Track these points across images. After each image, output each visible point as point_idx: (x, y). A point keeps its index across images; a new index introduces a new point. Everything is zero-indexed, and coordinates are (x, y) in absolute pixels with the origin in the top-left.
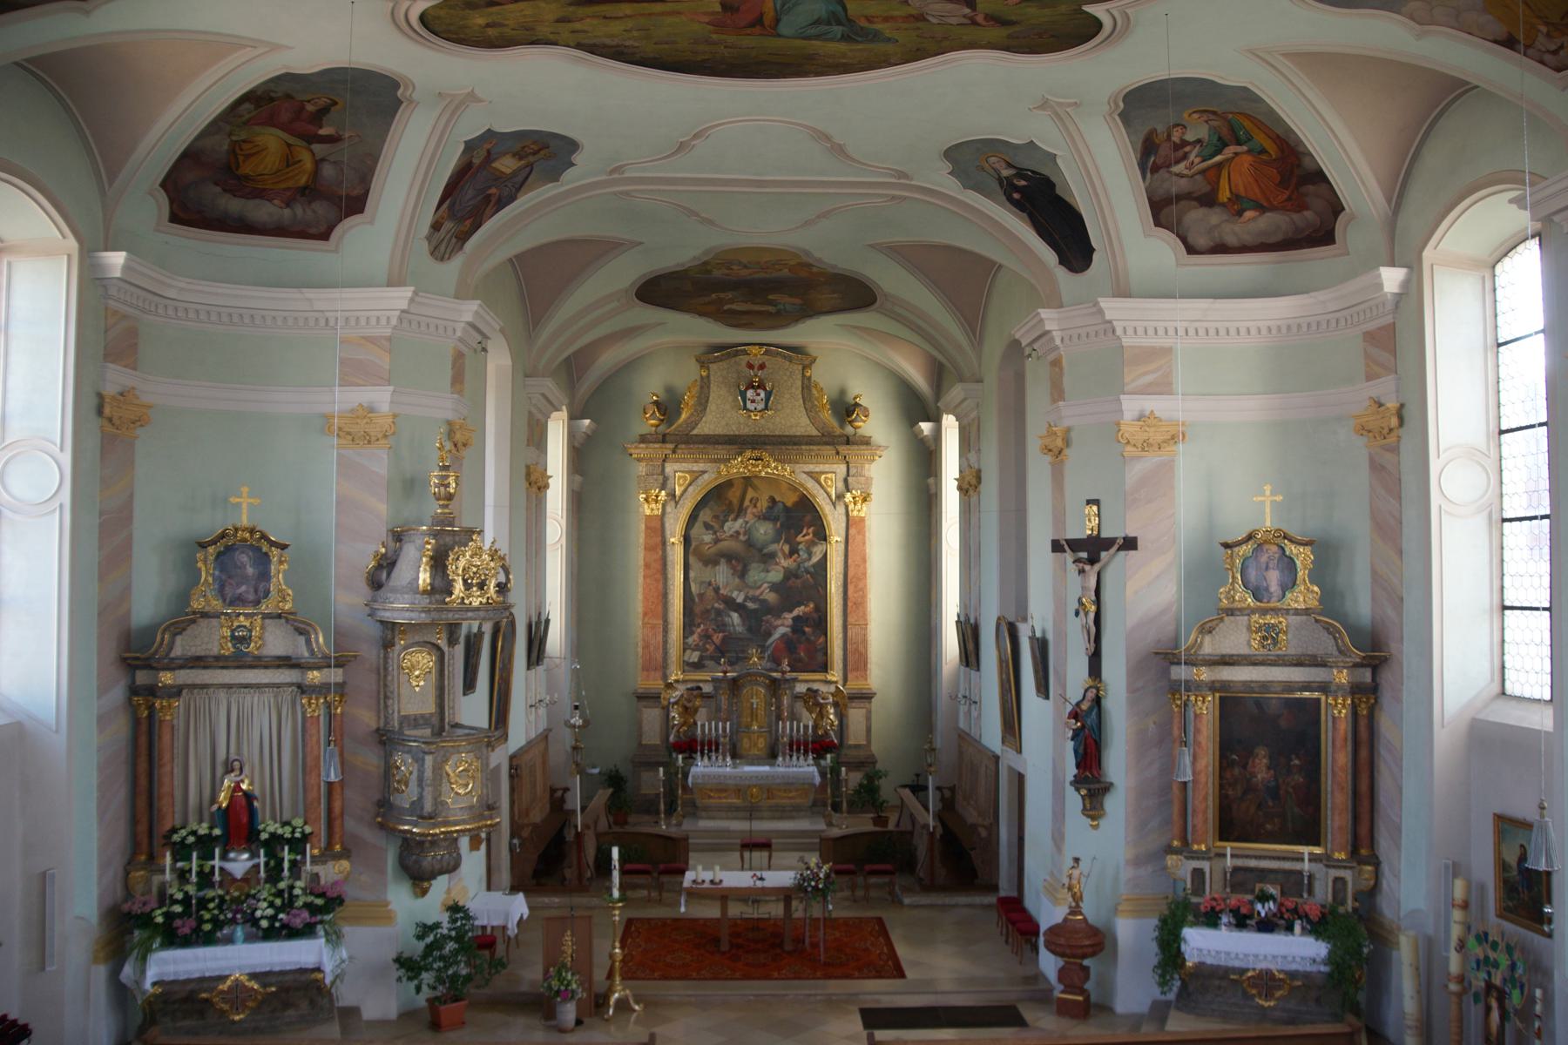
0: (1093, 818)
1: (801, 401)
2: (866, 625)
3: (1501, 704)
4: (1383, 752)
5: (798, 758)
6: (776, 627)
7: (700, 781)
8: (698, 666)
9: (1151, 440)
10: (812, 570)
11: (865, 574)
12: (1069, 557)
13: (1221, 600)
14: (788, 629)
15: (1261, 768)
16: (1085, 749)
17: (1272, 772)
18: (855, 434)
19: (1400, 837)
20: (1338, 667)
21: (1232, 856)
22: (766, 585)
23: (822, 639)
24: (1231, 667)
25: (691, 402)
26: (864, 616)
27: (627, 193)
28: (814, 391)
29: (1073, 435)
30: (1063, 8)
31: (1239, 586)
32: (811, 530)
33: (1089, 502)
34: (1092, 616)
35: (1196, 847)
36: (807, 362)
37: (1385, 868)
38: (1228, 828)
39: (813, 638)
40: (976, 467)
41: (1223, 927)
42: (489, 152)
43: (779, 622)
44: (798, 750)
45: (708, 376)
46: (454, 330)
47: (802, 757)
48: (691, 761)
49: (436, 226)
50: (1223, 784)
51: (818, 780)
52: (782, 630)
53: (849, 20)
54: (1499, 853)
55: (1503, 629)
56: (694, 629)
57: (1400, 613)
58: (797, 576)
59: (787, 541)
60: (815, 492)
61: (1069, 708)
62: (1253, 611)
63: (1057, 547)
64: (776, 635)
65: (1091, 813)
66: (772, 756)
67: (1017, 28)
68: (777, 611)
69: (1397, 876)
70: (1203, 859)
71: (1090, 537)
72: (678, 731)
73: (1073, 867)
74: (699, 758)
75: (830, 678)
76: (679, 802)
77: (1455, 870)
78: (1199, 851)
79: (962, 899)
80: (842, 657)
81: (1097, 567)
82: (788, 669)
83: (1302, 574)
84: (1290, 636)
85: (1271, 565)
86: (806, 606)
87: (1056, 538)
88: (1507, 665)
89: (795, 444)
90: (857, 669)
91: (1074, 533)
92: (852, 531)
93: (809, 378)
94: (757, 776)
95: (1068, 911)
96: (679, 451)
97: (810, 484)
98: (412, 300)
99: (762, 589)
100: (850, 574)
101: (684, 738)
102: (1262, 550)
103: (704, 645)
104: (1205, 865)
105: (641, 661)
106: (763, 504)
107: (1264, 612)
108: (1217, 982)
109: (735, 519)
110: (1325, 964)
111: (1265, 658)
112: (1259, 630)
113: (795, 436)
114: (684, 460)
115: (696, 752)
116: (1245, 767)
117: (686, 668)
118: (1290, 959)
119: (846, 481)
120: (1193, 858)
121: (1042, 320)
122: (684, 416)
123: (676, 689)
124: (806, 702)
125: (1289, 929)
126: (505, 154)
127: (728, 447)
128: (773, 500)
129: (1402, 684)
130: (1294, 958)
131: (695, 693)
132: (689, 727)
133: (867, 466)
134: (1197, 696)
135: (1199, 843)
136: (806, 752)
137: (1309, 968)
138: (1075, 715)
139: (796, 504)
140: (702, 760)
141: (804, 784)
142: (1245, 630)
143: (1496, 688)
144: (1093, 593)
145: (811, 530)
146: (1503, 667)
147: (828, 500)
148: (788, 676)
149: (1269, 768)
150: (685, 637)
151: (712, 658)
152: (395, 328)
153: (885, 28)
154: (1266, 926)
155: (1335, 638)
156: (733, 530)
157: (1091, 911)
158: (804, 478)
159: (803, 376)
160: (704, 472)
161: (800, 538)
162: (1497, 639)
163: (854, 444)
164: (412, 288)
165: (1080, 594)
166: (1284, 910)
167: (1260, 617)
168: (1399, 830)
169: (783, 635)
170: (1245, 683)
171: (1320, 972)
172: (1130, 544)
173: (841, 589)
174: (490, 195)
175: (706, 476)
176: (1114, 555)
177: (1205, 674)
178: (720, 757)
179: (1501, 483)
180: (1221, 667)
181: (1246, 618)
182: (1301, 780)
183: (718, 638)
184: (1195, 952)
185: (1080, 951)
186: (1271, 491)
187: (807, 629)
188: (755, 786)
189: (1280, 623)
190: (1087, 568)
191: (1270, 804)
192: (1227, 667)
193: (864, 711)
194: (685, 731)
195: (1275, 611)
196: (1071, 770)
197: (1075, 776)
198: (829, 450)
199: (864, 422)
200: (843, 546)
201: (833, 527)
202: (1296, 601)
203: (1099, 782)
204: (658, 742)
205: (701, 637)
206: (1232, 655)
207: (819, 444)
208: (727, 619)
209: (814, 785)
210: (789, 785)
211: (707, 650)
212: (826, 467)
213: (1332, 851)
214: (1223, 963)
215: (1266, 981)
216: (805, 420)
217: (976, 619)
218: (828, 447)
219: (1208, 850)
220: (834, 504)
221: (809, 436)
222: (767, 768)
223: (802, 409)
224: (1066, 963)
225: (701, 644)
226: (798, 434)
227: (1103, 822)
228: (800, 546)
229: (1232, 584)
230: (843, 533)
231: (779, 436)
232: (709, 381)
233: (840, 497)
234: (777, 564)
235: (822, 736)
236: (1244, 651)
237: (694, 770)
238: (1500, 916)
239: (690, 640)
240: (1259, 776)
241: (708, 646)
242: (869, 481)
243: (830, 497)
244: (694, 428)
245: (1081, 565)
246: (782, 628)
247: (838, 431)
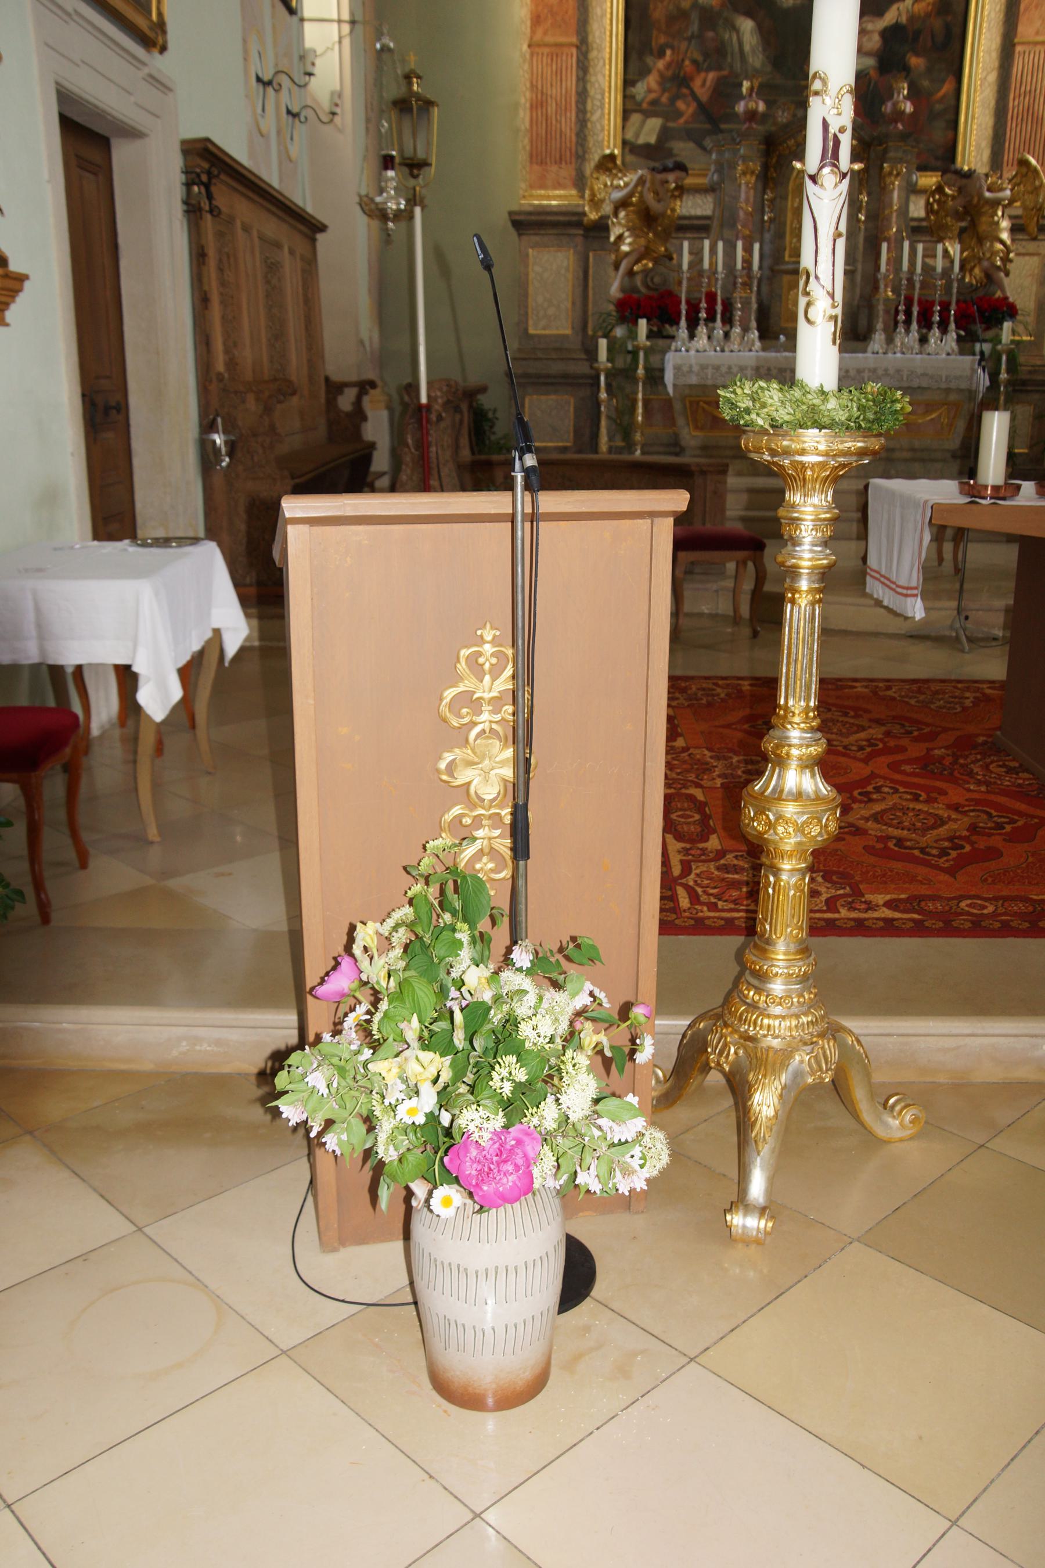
5: (923, 340)
39: (926, 83)
44: (926, 322)
47: (936, 332)
48: (661, 342)
56: (649, 60)
72: (631, 273)
74: (683, 332)
76: (638, 437)
80: (989, 132)
101: (643, 290)
103: (673, 100)
105: (526, 141)
115: (676, 322)
132: (656, 261)
140: (692, 336)
141: (948, 391)
150: (628, 83)
178: (737, 330)
183: (704, 84)
193: (1036, 259)
194: (646, 272)
204: (568, 332)
205: (663, 80)
211: (679, 114)
225: (664, 99)
237: (671, 360)
239: (640, 90)
241: (681, 105)
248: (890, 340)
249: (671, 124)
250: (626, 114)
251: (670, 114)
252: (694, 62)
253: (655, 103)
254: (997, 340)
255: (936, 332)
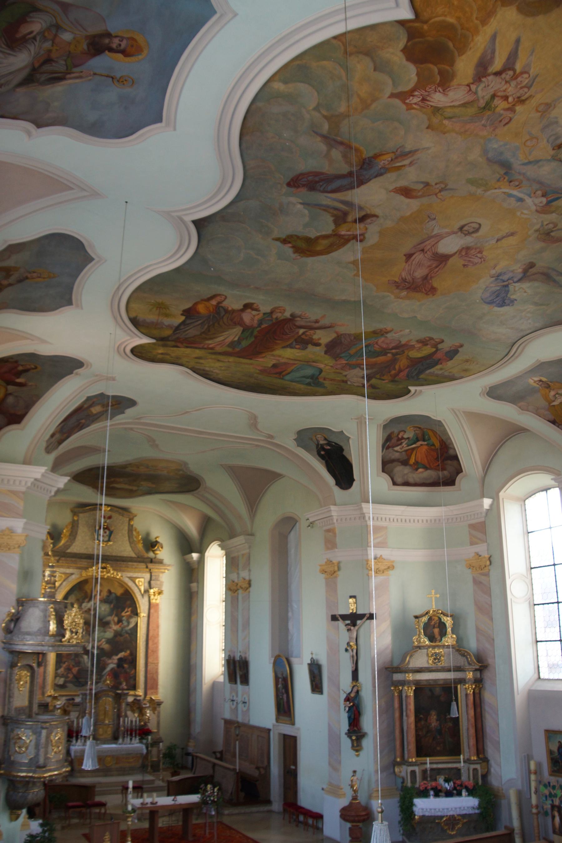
0: (357, 751)
1: (127, 538)
2: (158, 663)
3: (539, 682)
4: (487, 708)
5: (131, 739)
6: (108, 664)
7: (78, 754)
8: (62, 687)
9: (380, 569)
10: (129, 632)
11: (158, 635)
12: (341, 624)
13: (414, 642)
14: (115, 666)
15: (433, 720)
16: (354, 716)
17: (438, 722)
18: (155, 558)
19: (499, 747)
20: (468, 671)
21: (430, 763)
22: (104, 640)
23: (133, 672)
24: (421, 674)
25: (68, 534)
26: (157, 658)
27: (132, 429)
28: (134, 533)
29: (341, 565)
30: (401, 386)
31: (422, 636)
32: (130, 609)
33: (351, 597)
34: (355, 651)
35: (410, 760)
36: (131, 517)
37: (492, 762)
38: (421, 751)
39: (128, 671)
40: (247, 578)
41: (432, 797)
42: (93, 403)
43: (110, 661)
44: (131, 735)
45: (78, 520)
46: (51, 491)
49: (52, 436)
50: (417, 729)
51: (145, 751)
52: (111, 666)
53: (317, 378)
54: (548, 747)
55: (537, 651)
57: (493, 645)
58: (121, 635)
59: (116, 615)
60: (133, 588)
61: (344, 696)
62: (429, 647)
63: (334, 618)
64: (108, 669)
65: (357, 748)
66: (115, 738)
67: (377, 390)
68: (109, 655)
69: (499, 765)
70: (415, 765)
71: (352, 614)
73: (353, 776)
74: (74, 741)
75: (137, 693)
77: (529, 758)
78: (412, 762)
79: (254, 809)
81: (357, 628)
82: (125, 687)
83: (449, 630)
84: (445, 658)
85: (436, 626)
86: (125, 652)
87: (334, 614)
88: (540, 666)
89: (123, 561)
90: (152, 688)
91: (342, 611)
92: (152, 611)
93: (132, 526)
94: (111, 750)
95: (351, 798)
96: (61, 561)
97: (130, 584)
98: (43, 475)
99: (101, 642)
100: (151, 634)
102: (432, 620)
104: (416, 769)
106: (105, 594)
107: (434, 647)
108: (430, 825)
109: (89, 602)
110: (478, 809)
111: (435, 668)
112: (432, 655)
113: (123, 557)
114: (62, 567)
116: (426, 720)
117: (56, 688)
118: (462, 808)
119: (150, 583)
120: (410, 765)
121: (330, 511)
122: (63, 542)
123: (59, 700)
124: (131, 707)
125: (459, 794)
126: (98, 404)
127: (89, 561)
128: (110, 592)
129: (496, 677)
130: (464, 808)
131: (71, 702)
133: (161, 575)
134: (408, 687)
135: (412, 758)
136: (135, 737)
137: (471, 812)
138: (347, 699)
139: (122, 594)
142: (426, 656)
143: (536, 676)
144: (355, 640)
145: (130, 609)
146: (538, 667)
147: (139, 593)
148: (126, 692)
149: (437, 720)
150: (57, 669)
151: (71, 682)
152: (28, 488)
153: (327, 383)
154: (449, 794)
155: (467, 658)
156: (87, 608)
157: (362, 799)
158: (127, 581)
159: (129, 524)
160: (72, 574)
161: (123, 614)
162: (535, 655)
163: (155, 563)
164: (46, 468)
165: (348, 640)
166: (456, 785)
167: (432, 649)
168: (498, 743)
169: (112, 669)
170: (427, 680)
171: (475, 813)
172: (371, 617)
173: (145, 643)
174: (80, 423)
175: (73, 576)
176: (364, 622)
177: (411, 677)
179: (533, 589)
180: (416, 674)
181: (426, 650)
182: (451, 725)
183: (75, 670)
184: (420, 810)
185: (362, 818)
186: (435, 593)
187: (126, 666)
188: (110, 756)
189: (441, 652)
190: (352, 628)
191: (438, 737)
192: (418, 674)
195: (439, 647)
196: (345, 726)
197: (348, 730)
198: (143, 565)
199: (160, 551)
200: (146, 619)
201: (142, 608)
202: (447, 642)
203: (360, 732)
206: (422, 668)
207: (136, 562)
208: (81, 659)
209: (142, 754)
210: (129, 755)
211: (68, 677)
212: (139, 575)
213: (470, 756)
214: (433, 815)
215: (452, 821)
216: (129, 548)
217: (246, 658)
218: (142, 564)
219: (416, 762)
220: (143, 595)
221: (131, 557)
222: (114, 746)
223: (128, 542)
224: (353, 826)
225: (65, 674)
226: (125, 555)
227: (362, 753)
228: (124, 618)
229: (419, 635)
230: (147, 611)
231: (115, 556)
232: (78, 523)
233: (146, 591)
234: (110, 628)
235: (142, 726)
236: (426, 665)
238: (551, 775)
240: (433, 724)
241: (69, 675)
242: (162, 583)
243: (140, 591)
244: (68, 549)
245: (349, 627)
246: (112, 664)
247: (146, 555)
248: (123, 740)
249: (67, 680)
250: (56, 677)
251: (67, 677)
252: (73, 665)
253: (63, 675)
254: (147, 739)
255: (134, 738)
